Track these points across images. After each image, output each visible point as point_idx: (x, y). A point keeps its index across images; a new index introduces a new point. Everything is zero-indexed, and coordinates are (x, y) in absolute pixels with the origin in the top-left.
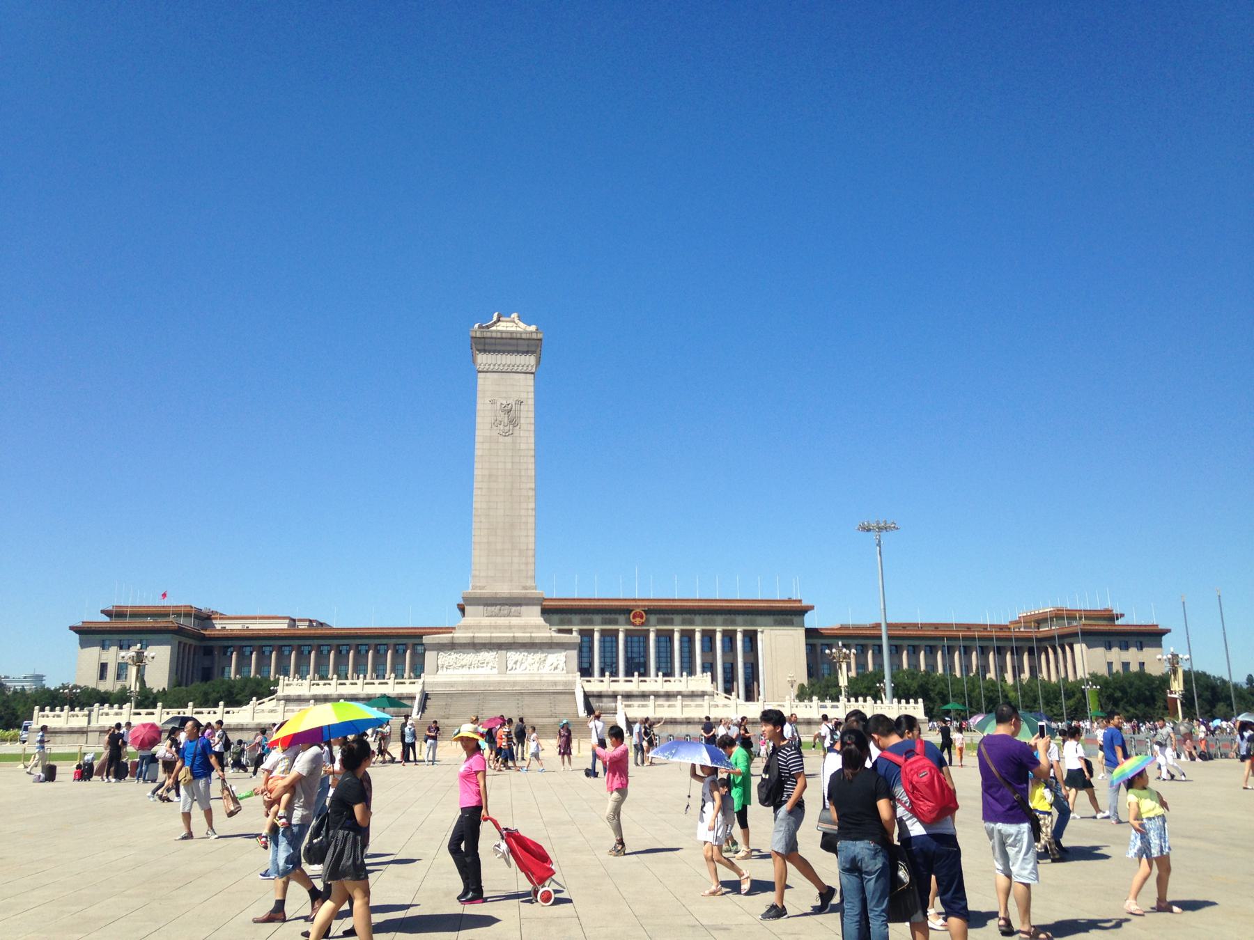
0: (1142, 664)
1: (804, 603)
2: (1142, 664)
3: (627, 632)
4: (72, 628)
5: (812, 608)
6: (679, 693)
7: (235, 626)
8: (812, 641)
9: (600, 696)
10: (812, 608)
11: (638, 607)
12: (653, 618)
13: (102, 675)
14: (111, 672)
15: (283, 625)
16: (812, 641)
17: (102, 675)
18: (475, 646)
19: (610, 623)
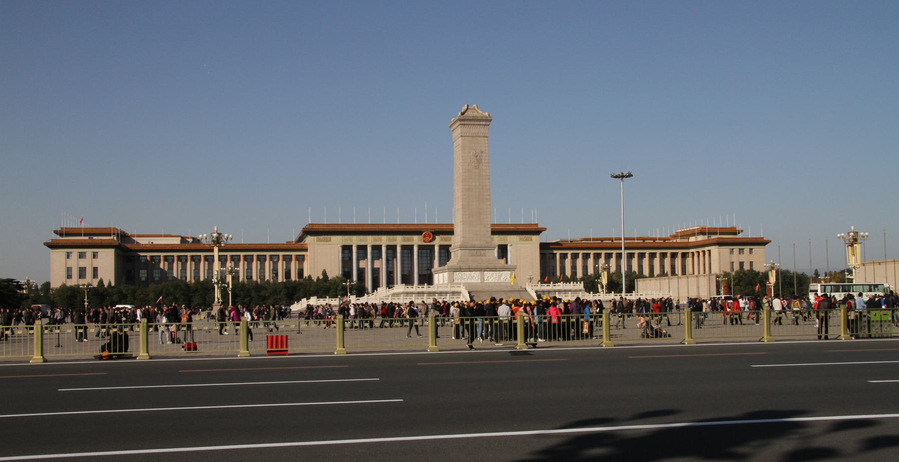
0: (751, 263)
1: (540, 226)
2: (751, 263)
3: (420, 247)
4: (46, 244)
5: (545, 229)
6: (570, 291)
7: (144, 241)
8: (543, 252)
9: (543, 292)
10: (545, 229)
11: (427, 230)
12: (437, 237)
13: (69, 276)
14: (89, 273)
15: (177, 241)
16: (543, 252)
17: (69, 276)
18: (470, 270)
19: (408, 240)
